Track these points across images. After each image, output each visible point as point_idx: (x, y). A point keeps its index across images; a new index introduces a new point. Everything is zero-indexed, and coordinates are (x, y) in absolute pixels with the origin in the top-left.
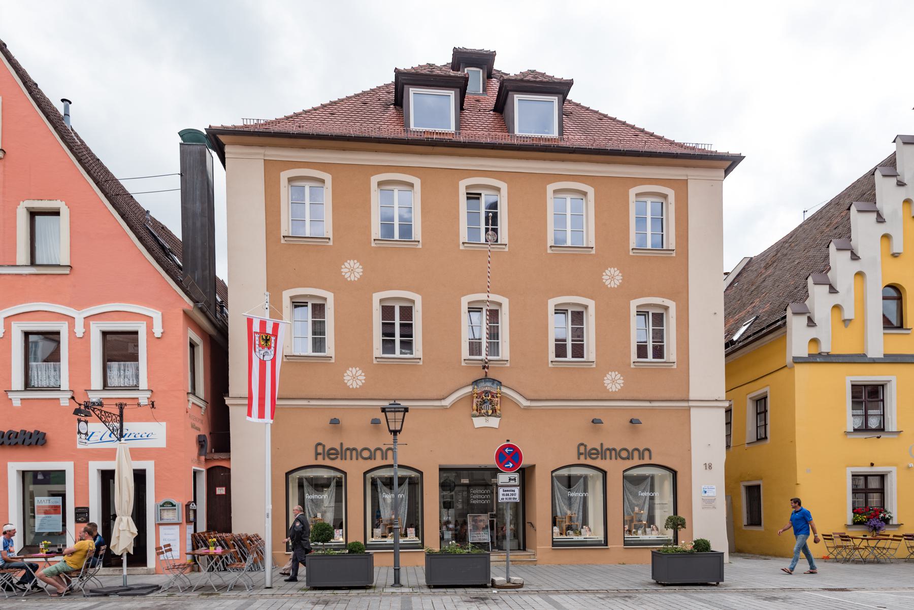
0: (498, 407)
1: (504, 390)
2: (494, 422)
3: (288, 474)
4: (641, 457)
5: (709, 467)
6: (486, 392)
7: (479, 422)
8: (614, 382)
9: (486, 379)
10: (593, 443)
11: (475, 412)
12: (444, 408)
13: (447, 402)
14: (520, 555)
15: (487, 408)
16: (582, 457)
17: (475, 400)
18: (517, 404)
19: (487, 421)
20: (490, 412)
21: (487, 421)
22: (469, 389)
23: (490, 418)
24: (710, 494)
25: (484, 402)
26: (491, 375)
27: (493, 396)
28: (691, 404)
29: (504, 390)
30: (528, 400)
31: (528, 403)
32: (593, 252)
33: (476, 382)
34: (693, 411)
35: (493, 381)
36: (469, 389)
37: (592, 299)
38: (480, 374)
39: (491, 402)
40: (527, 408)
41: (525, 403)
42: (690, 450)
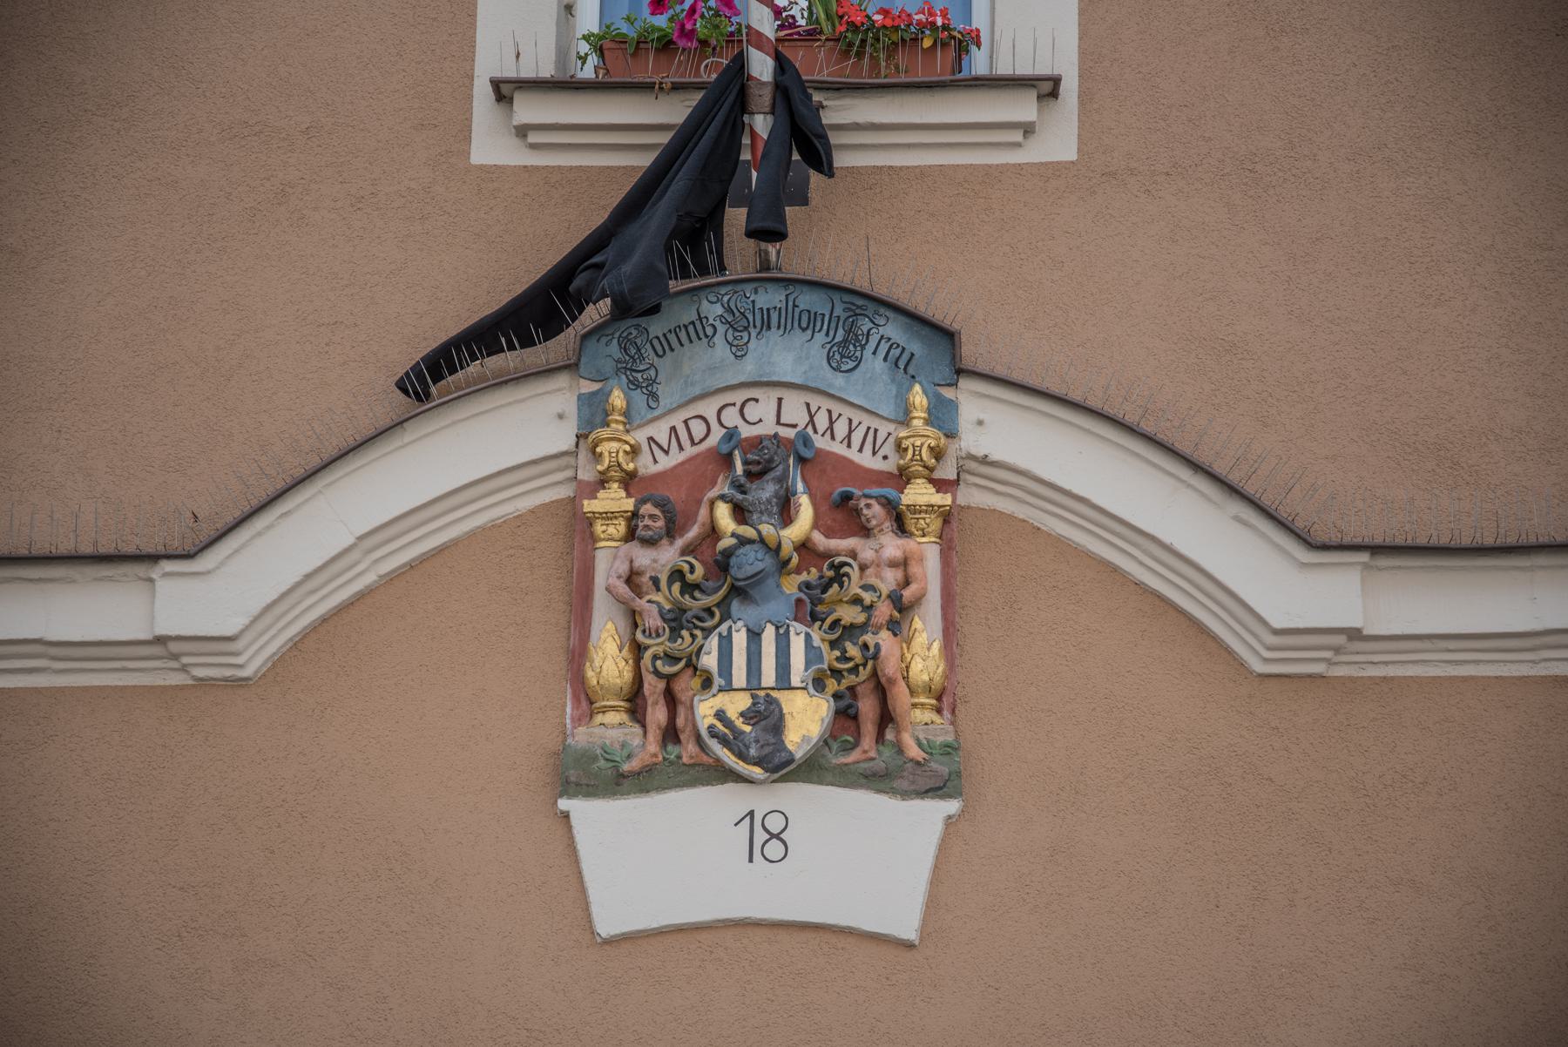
0: (921, 655)
2: (864, 859)
6: (759, 466)
7: (658, 859)
11: (613, 727)
15: (771, 666)
17: (608, 564)
19: (764, 840)
20: (806, 718)
21: (764, 840)
23: (806, 804)
25: (721, 583)
27: (844, 513)
29: (994, 428)
31: (1329, 597)
35: (850, 312)
39: (822, 587)
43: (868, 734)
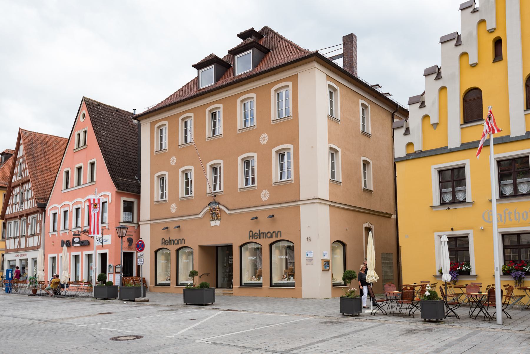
1: (221, 207)
2: (218, 223)
3: (156, 252)
4: (277, 236)
5: (309, 239)
6: (214, 209)
7: (213, 223)
8: (265, 195)
9: (215, 202)
10: (256, 231)
12: (200, 218)
13: (200, 216)
14: (227, 291)
16: (251, 238)
18: (226, 213)
20: (216, 218)
22: (208, 208)
24: (310, 256)
25: (212, 214)
26: (217, 199)
28: (299, 203)
30: (228, 209)
32: (256, 128)
33: (209, 204)
34: (302, 207)
36: (208, 208)
37: (255, 152)
38: (212, 200)
40: (230, 214)
41: (228, 212)
42: (300, 230)
43: (217, 219)
